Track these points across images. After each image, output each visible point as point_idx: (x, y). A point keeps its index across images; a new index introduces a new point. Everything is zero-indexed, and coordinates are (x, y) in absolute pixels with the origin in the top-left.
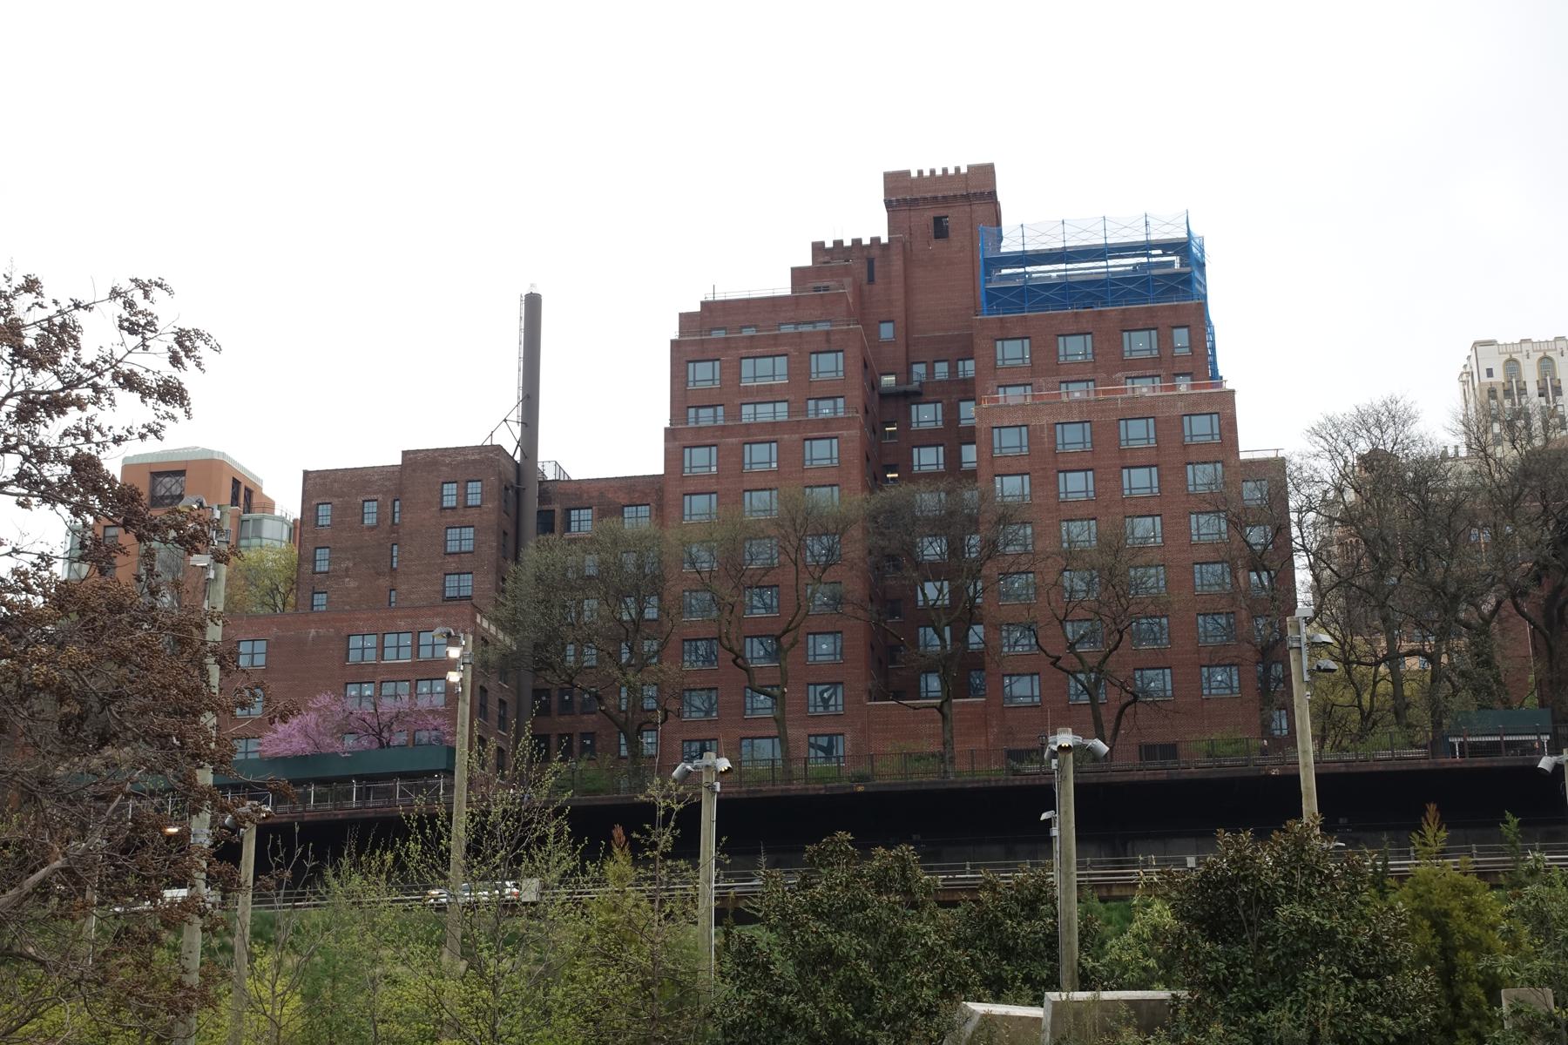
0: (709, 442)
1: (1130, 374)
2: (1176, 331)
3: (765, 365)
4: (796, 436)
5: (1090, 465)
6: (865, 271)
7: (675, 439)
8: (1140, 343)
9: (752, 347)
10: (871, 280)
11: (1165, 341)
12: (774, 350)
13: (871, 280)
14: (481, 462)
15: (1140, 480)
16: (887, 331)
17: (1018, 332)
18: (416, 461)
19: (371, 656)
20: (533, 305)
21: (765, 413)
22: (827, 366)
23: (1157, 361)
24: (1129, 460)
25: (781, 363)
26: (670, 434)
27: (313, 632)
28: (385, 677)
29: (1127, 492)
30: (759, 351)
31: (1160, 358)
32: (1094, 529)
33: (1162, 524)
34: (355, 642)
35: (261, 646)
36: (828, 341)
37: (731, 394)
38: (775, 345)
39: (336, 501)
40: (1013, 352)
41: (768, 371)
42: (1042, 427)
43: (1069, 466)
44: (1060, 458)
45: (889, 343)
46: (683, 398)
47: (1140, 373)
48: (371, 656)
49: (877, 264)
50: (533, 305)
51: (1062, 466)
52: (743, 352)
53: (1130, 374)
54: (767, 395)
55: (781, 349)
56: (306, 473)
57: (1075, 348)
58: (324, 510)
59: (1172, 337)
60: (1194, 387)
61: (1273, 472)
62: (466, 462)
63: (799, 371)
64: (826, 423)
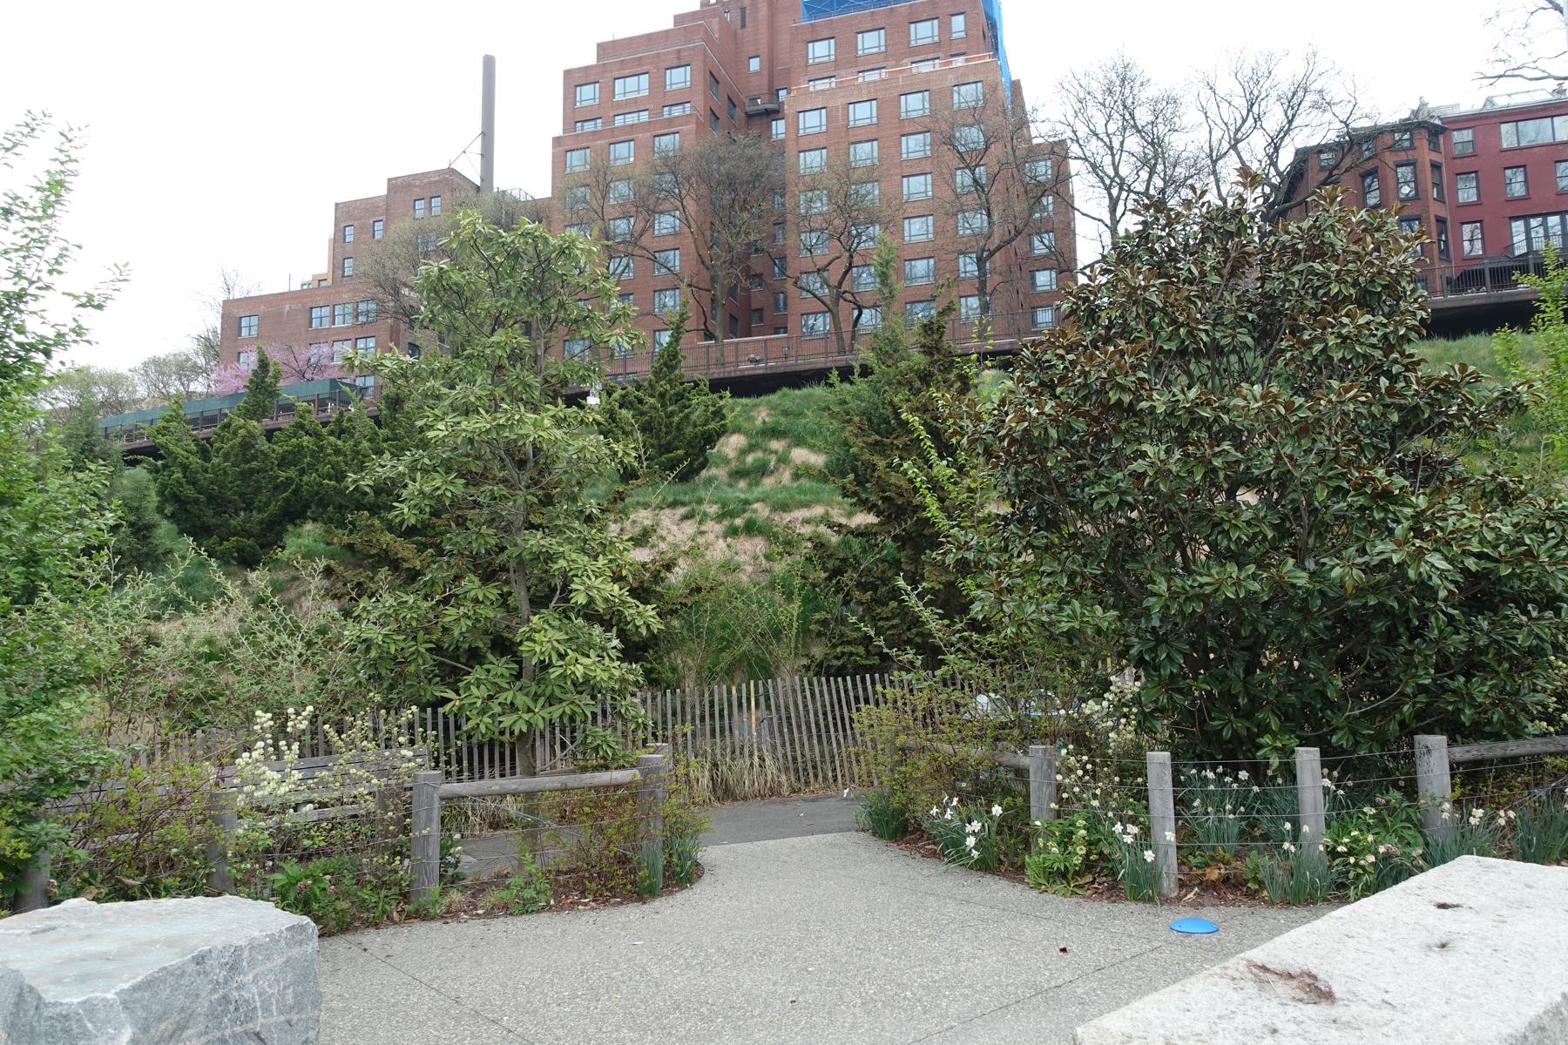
0: (584, 145)
1: (914, 59)
2: (954, 19)
3: (632, 83)
4: (648, 134)
5: (874, 136)
6: (739, 18)
7: (560, 145)
8: (924, 32)
9: (623, 69)
10: (743, 26)
11: (945, 28)
12: (639, 70)
13: (743, 26)
14: (440, 182)
15: (914, 146)
16: (755, 65)
17: (825, 34)
18: (396, 186)
19: (326, 325)
20: (489, 64)
21: (631, 119)
22: (678, 78)
23: (937, 46)
24: (907, 128)
25: (644, 79)
26: (557, 141)
27: (287, 307)
28: (335, 338)
29: (904, 156)
30: (627, 72)
31: (939, 43)
32: (824, 156)
33: (879, 149)
34: (316, 312)
35: (254, 320)
36: (679, 58)
37: (609, 106)
38: (640, 65)
39: (356, 223)
40: (821, 51)
41: (633, 87)
42: (837, 108)
43: (859, 138)
44: (851, 132)
45: (756, 73)
46: (573, 116)
47: (923, 57)
48: (326, 325)
49: (747, 12)
50: (489, 64)
51: (852, 140)
52: (617, 74)
53: (914, 59)
54: (634, 106)
55: (645, 68)
56: (337, 204)
57: (871, 42)
58: (349, 231)
59: (950, 24)
60: (967, 60)
61: (1057, 152)
62: (430, 183)
63: (658, 85)
64: (671, 121)
